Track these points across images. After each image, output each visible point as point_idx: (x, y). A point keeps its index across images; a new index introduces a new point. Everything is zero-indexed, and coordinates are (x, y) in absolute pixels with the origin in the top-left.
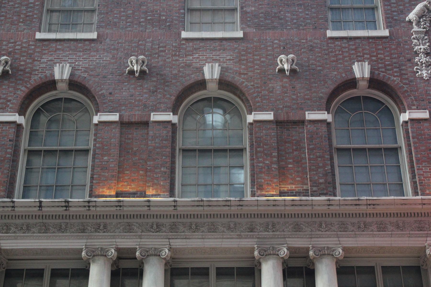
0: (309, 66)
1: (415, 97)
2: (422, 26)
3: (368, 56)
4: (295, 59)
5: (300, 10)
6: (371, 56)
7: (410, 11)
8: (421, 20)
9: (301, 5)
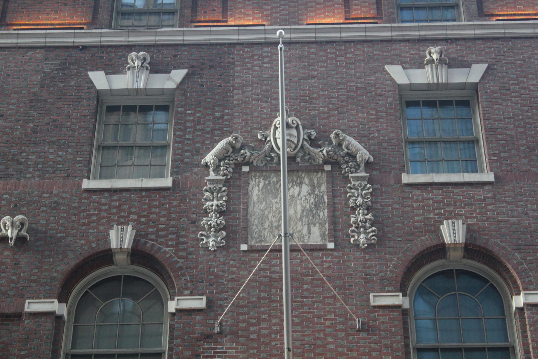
0: (46, 232)
1: (191, 276)
2: (221, 172)
3: (135, 217)
4: (25, 221)
5: (51, 151)
6: (140, 217)
7: (209, 150)
8: (222, 163)
9: (53, 142)
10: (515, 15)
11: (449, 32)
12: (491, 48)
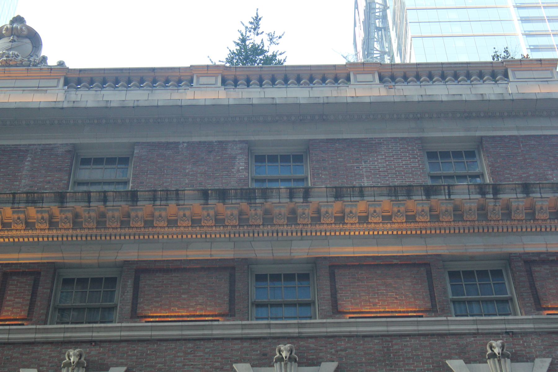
10: (167, 317)
11: (95, 334)
12: (135, 350)
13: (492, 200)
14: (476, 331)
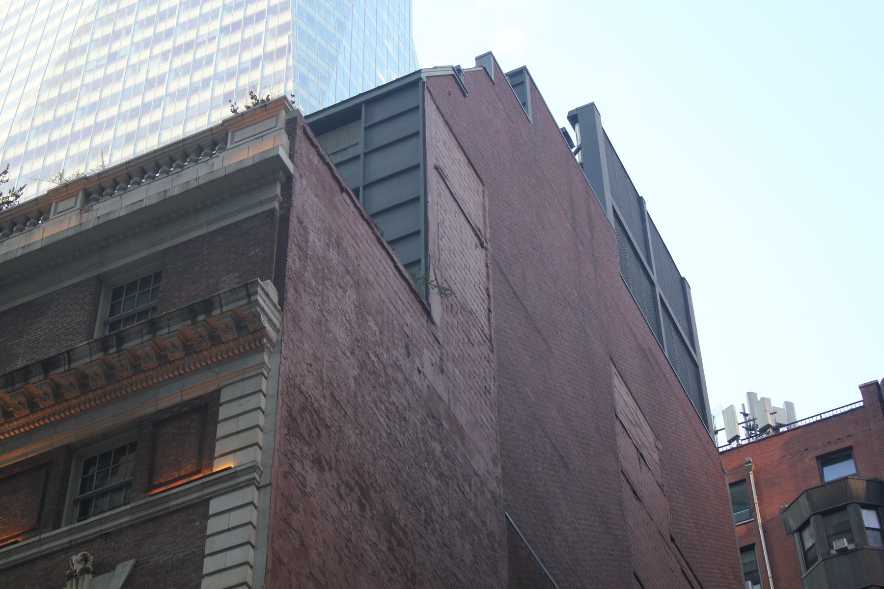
13: (115, 355)
14: (69, 545)
